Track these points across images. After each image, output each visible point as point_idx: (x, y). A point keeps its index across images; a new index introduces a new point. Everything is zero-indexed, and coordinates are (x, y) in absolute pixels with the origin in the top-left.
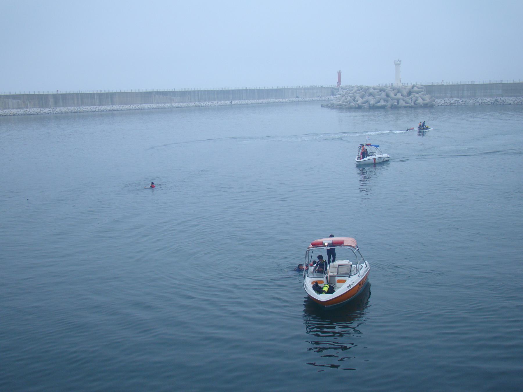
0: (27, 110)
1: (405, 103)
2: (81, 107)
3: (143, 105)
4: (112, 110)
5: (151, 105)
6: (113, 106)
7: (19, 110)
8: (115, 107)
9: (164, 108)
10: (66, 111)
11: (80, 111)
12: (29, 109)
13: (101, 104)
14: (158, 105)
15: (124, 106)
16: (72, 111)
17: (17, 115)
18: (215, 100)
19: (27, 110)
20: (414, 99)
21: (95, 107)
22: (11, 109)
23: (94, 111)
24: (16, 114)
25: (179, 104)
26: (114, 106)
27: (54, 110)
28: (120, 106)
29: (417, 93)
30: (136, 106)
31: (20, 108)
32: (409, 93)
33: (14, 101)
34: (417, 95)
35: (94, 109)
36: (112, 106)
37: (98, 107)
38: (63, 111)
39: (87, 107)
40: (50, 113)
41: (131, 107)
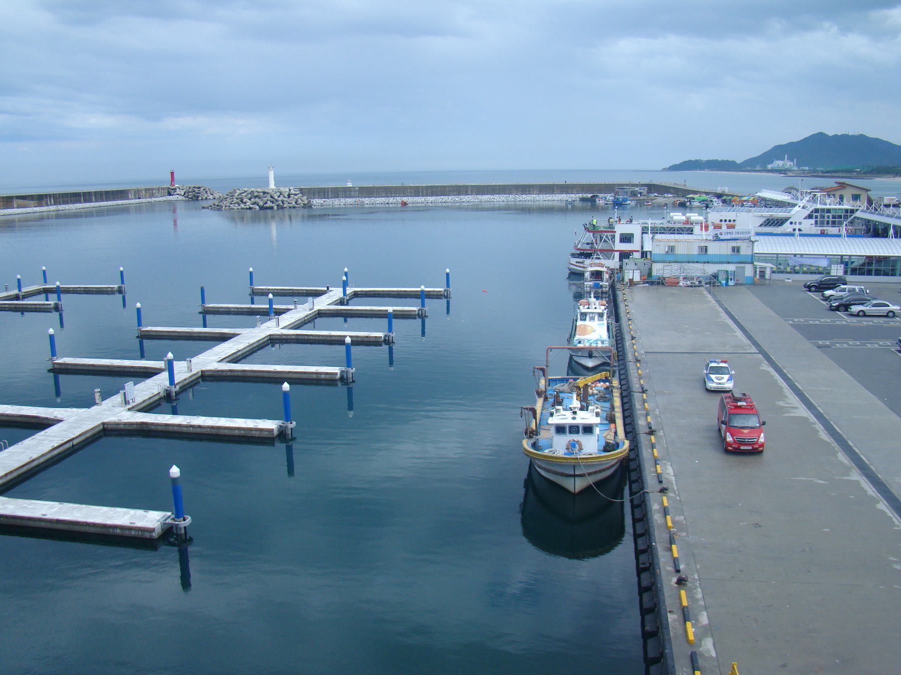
1: (289, 203)
20: (295, 200)
29: (296, 195)
32: (289, 196)
34: (296, 197)
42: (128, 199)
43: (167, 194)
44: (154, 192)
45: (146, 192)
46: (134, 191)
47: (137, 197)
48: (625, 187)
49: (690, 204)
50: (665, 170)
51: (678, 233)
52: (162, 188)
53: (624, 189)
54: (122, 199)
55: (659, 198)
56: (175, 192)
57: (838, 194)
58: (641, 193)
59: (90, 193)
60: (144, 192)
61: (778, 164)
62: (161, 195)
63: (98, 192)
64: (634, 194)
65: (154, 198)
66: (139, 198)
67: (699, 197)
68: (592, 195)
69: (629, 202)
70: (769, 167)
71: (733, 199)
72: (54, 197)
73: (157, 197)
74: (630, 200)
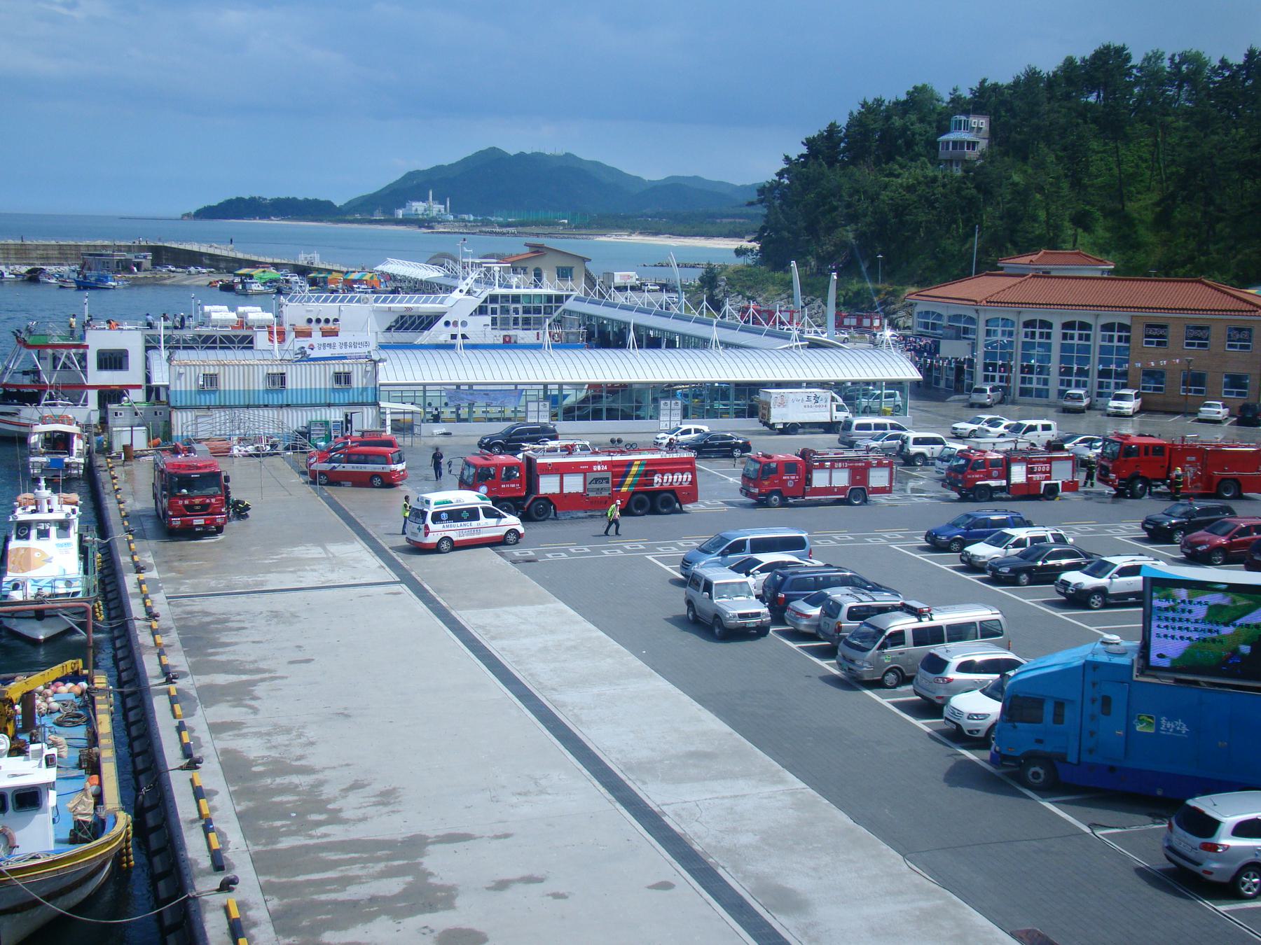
48: (104, 252)
49: (244, 287)
50: (187, 216)
51: (221, 348)
53: (101, 255)
55: (179, 276)
57: (531, 267)
58: (139, 266)
61: (418, 207)
64: (126, 266)
67: (262, 274)
68: (29, 268)
69: (113, 284)
70: (400, 213)
71: (330, 277)
74: (114, 281)
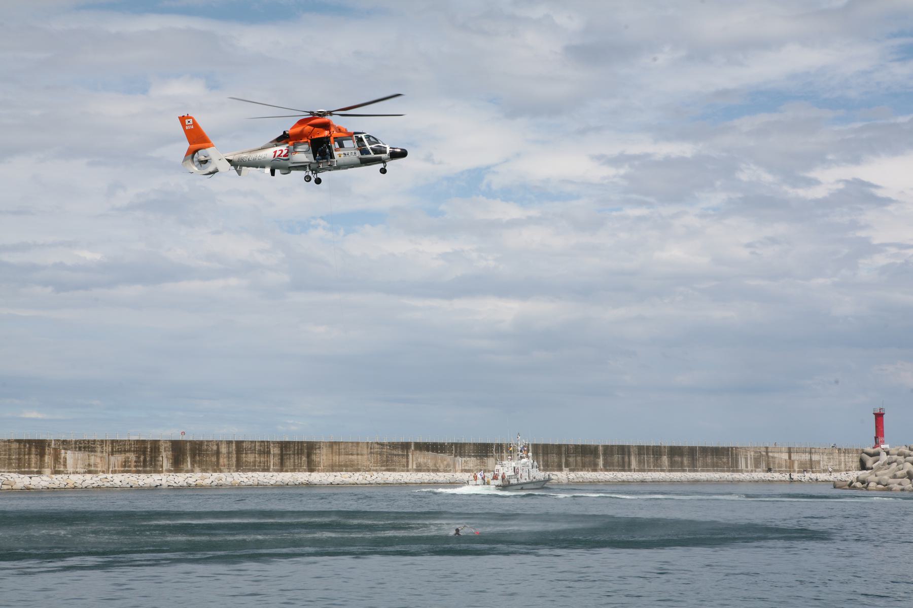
0: (106, 478)
2: (236, 475)
3: (384, 473)
4: (309, 485)
5: (403, 474)
6: (312, 473)
7: (88, 476)
8: (316, 477)
9: (435, 483)
10: (197, 482)
11: (233, 482)
12: (111, 475)
13: (282, 468)
14: (420, 475)
15: (338, 474)
16: (212, 482)
17: (82, 488)
18: (561, 470)
19: (106, 478)
21: (268, 475)
22: (70, 474)
23: (264, 484)
24: (80, 486)
25: (471, 475)
26: (314, 474)
27: (171, 478)
28: (327, 473)
30: (366, 475)
31: (90, 472)
33: (80, 455)
35: (265, 480)
36: (309, 473)
37: (275, 474)
38: (191, 482)
39: (250, 474)
40: (161, 485)
41: (356, 478)
42: (734, 468)
43: (856, 464)
44: (815, 457)
45: (790, 457)
46: (755, 452)
47: (763, 465)
52: (839, 449)
54: (715, 467)
56: (875, 463)
59: (624, 450)
60: (785, 456)
62: (837, 468)
63: (648, 447)
65: (813, 472)
66: (769, 470)
72: (456, 447)
73: (825, 471)
